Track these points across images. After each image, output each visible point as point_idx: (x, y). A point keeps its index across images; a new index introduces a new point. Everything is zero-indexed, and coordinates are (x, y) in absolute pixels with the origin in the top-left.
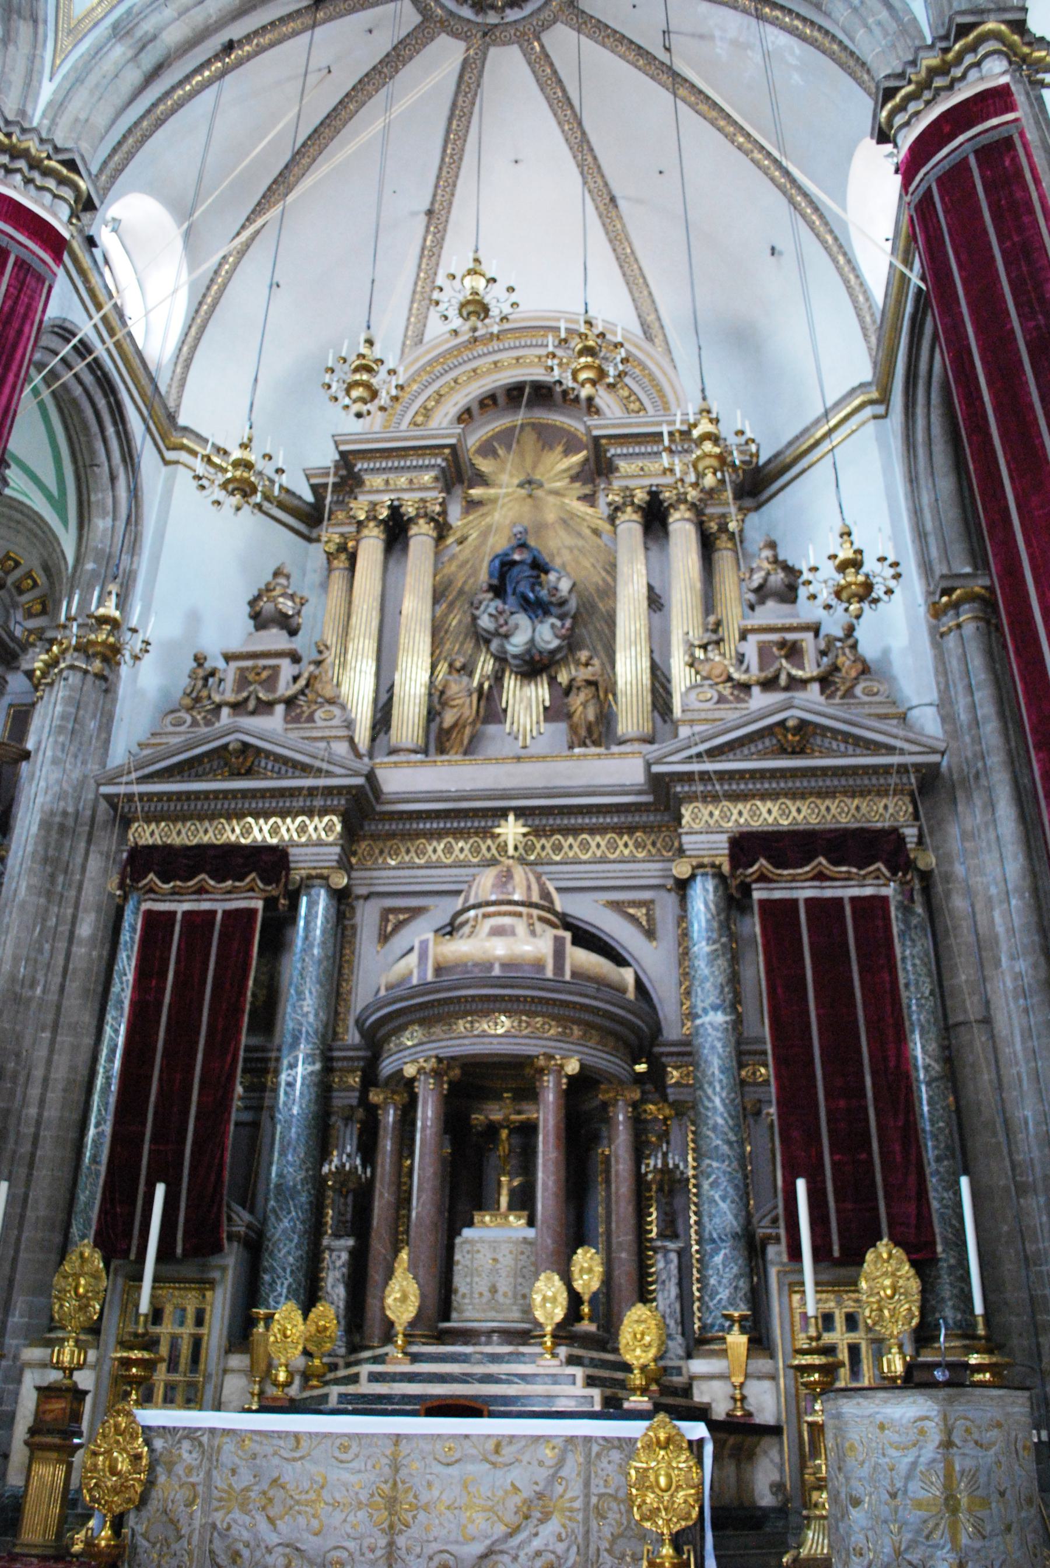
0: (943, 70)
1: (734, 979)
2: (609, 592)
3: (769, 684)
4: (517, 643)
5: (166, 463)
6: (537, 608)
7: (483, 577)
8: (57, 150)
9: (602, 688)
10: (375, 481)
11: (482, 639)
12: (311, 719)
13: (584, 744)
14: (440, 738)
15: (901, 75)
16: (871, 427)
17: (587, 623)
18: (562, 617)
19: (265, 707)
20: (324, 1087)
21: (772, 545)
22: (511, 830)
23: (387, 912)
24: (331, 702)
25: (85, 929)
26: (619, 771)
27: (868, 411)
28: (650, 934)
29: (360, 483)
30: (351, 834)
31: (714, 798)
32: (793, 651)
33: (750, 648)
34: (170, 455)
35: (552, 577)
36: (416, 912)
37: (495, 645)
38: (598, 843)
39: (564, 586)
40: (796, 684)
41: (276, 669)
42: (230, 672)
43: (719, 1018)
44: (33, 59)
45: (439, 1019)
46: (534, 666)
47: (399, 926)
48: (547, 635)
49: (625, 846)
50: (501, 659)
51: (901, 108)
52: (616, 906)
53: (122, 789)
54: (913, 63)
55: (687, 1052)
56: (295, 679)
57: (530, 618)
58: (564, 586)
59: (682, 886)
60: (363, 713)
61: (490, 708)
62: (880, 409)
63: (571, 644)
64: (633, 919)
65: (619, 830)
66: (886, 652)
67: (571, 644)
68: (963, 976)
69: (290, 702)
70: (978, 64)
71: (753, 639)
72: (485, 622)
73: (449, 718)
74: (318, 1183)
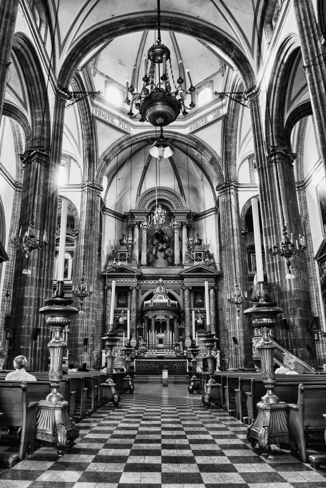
1: (190, 303)
2: (173, 237)
3: (197, 260)
4: (160, 247)
5: (104, 214)
6: (163, 242)
7: (154, 234)
8: (99, 186)
9: (173, 257)
10: (137, 217)
11: (154, 245)
12: (131, 262)
13: (170, 266)
14: (149, 264)
16: (214, 215)
17: (170, 243)
18: (166, 243)
19: (124, 260)
20: (137, 316)
21: (198, 235)
22: (161, 280)
23: (143, 290)
24: (134, 260)
25: (101, 293)
26: (175, 271)
27: (214, 213)
28: (179, 295)
29: (134, 217)
30: (138, 280)
31: (188, 278)
32: (200, 255)
33: (194, 254)
34: (104, 212)
35: (165, 236)
36: (147, 291)
37: (156, 247)
38: (172, 282)
39: (167, 238)
40: (200, 260)
41: (126, 254)
42: (119, 253)
43: (188, 309)
44: (94, 169)
45: (154, 310)
46: (162, 250)
47: (144, 293)
48: (164, 247)
49: (176, 282)
50: (157, 248)
52: (174, 290)
53: (107, 274)
54: (222, 185)
55: (184, 312)
56: (129, 255)
57: (160, 239)
58: (167, 238)
59: (184, 290)
60: (137, 259)
61: (156, 257)
62: (216, 212)
63: (168, 247)
64: (177, 292)
65: (175, 280)
66: (213, 254)
67: (168, 247)
68: (219, 303)
69: (128, 259)
71: (195, 253)
72: (155, 243)
73: (150, 260)
74: (137, 328)
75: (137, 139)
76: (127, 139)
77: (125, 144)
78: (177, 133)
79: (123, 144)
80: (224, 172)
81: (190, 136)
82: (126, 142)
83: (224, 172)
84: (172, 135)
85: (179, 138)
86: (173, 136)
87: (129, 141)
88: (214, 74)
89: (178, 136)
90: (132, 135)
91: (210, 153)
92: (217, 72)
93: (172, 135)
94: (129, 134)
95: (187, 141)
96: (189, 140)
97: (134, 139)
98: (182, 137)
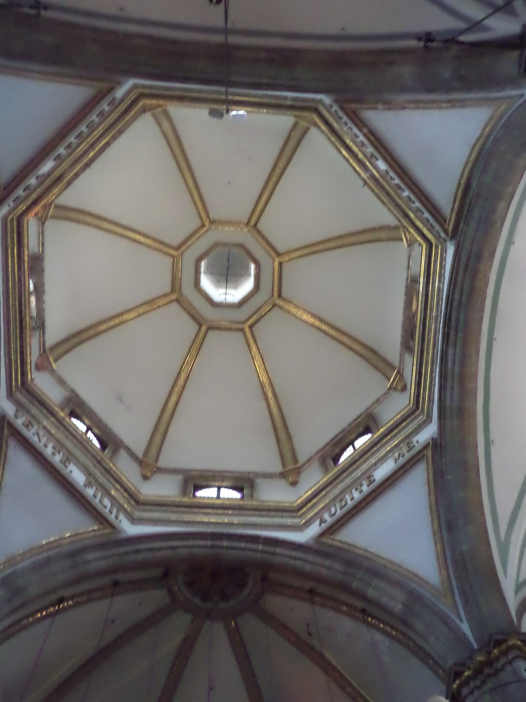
0: (489, 663)
15: (464, 665)
51: (466, 682)
54: (471, 658)
70: (510, 662)
75: (138, 551)
76: (102, 546)
77: (96, 561)
78: (276, 542)
79: (90, 556)
80: (465, 627)
81: (323, 544)
82: (99, 554)
83: (465, 627)
84: (260, 547)
85: (283, 556)
86: (263, 552)
87: (110, 552)
88: (378, 400)
89: (278, 550)
90: (123, 535)
91: (398, 584)
92: (385, 394)
93: (260, 547)
94: (112, 526)
95: (311, 564)
96: (319, 560)
97: (129, 548)
98: (294, 554)
